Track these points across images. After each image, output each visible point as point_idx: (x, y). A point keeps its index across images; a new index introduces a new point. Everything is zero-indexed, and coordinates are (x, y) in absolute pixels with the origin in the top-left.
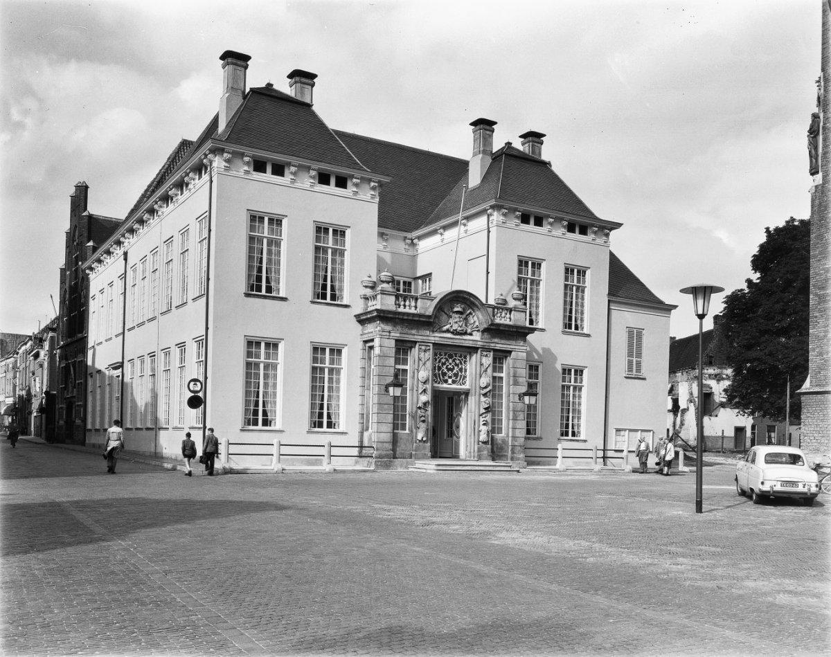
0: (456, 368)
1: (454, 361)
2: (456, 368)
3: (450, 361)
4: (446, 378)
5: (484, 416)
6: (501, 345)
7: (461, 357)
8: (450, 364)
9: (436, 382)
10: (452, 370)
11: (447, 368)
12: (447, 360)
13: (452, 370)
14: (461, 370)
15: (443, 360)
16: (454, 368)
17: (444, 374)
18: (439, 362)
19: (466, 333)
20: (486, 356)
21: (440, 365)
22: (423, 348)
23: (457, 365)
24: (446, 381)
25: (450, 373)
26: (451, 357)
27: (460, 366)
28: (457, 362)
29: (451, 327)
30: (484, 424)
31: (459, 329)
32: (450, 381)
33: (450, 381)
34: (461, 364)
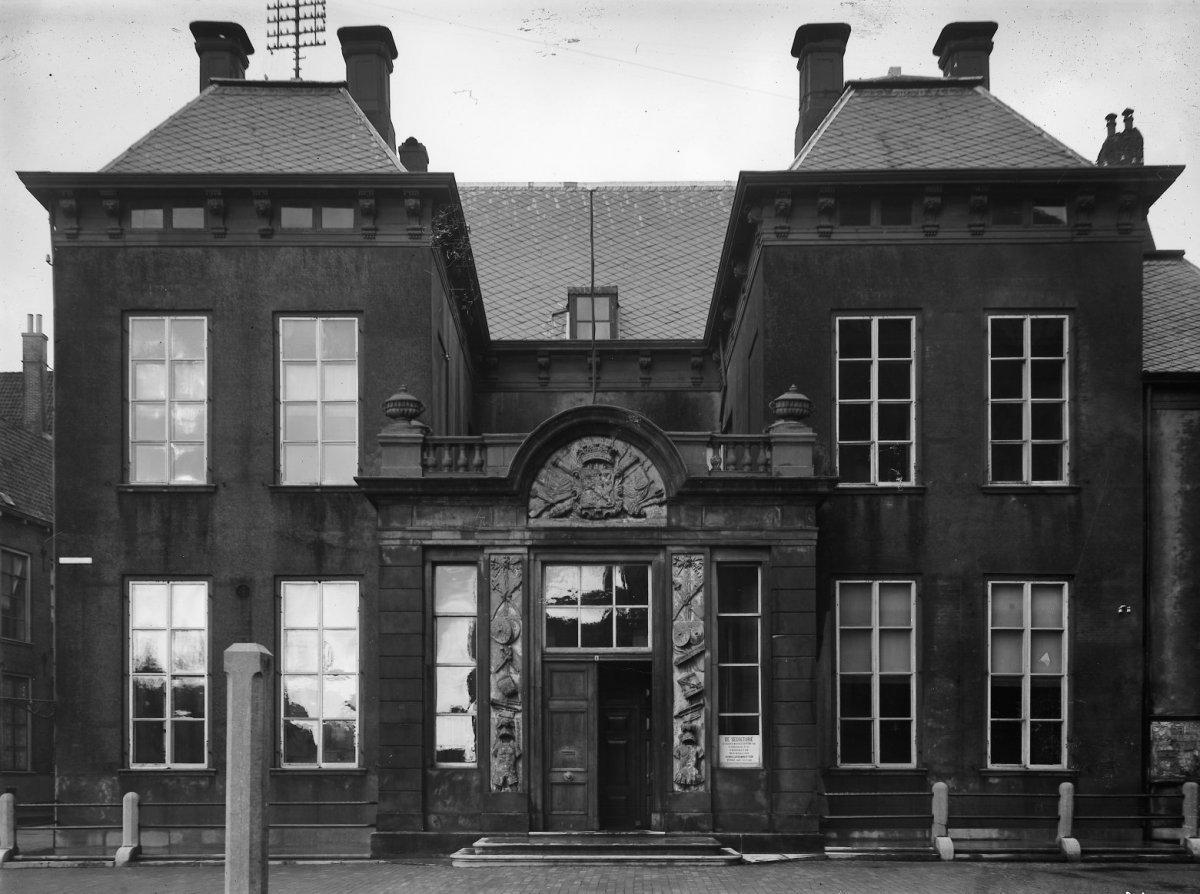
5: (687, 718)
19: (622, 513)
29: (577, 500)
30: (687, 742)
31: (600, 503)
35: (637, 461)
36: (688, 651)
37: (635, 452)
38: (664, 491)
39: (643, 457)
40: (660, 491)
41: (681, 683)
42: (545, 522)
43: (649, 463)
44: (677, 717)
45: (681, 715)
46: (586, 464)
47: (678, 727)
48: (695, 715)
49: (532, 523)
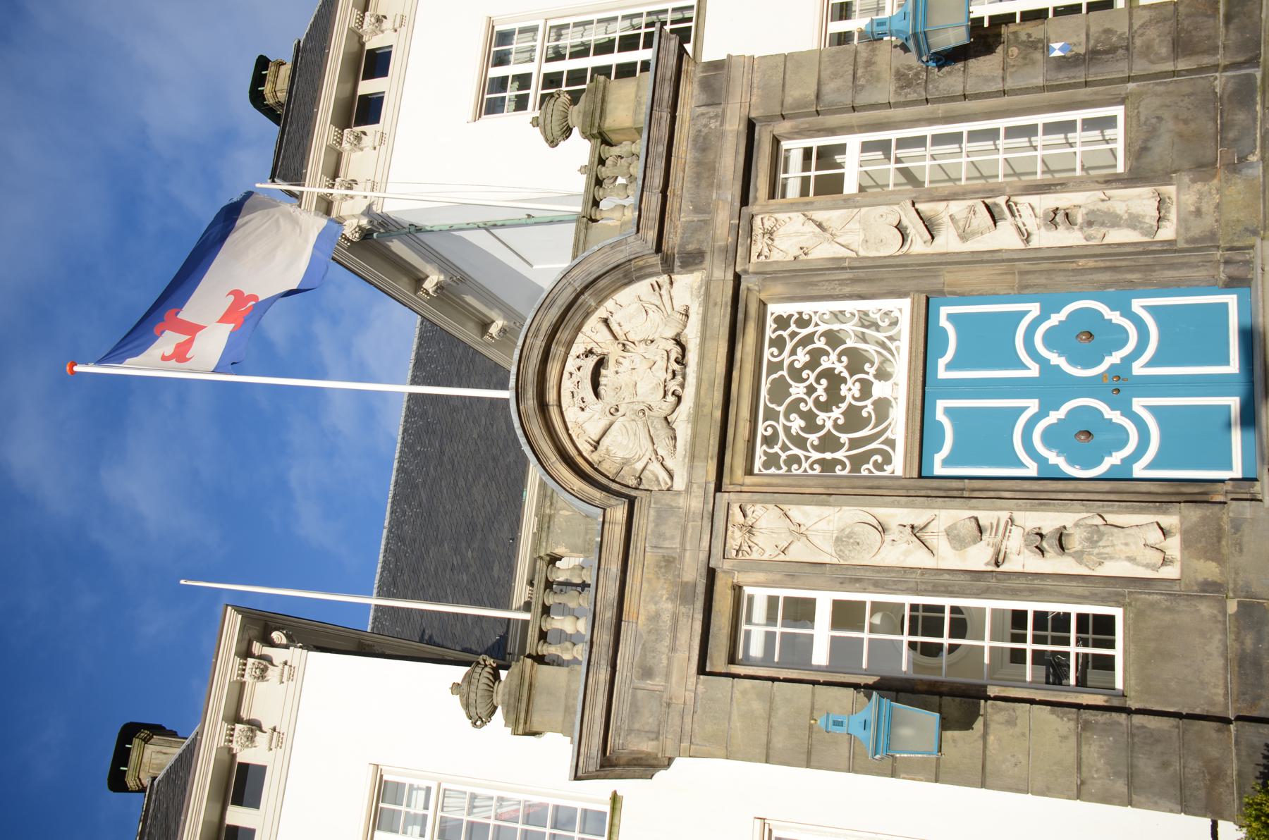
0: (825, 363)
1: (796, 375)
2: (825, 363)
3: (798, 390)
4: (868, 408)
5: (1031, 223)
6: (911, 44)
7: (779, 343)
8: (810, 390)
9: (888, 459)
10: (834, 381)
11: (825, 407)
12: (794, 407)
13: (834, 381)
14: (833, 339)
15: (797, 424)
16: (829, 374)
17: (854, 419)
18: (801, 443)
20: (770, 234)
21: (813, 438)
22: (736, 538)
23: (816, 356)
24: (883, 407)
25: (850, 390)
26: (780, 389)
27: (820, 343)
28: (802, 357)
32: (880, 389)
33: (880, 389)
34: (809, 339)
35: (606, 321)
36: (911, 232)
37: (593, 326)
38: (653, 280)
39: (601, 312)
40: (652, 285)
41: (964, 237)
42: (677, 463)
43: (609, 304)
44: (1027, 241)
45: (1027, 237)
46: (597, 395)
47: (1045, 239)
48: (1025, 211)
49: (679, 484)
